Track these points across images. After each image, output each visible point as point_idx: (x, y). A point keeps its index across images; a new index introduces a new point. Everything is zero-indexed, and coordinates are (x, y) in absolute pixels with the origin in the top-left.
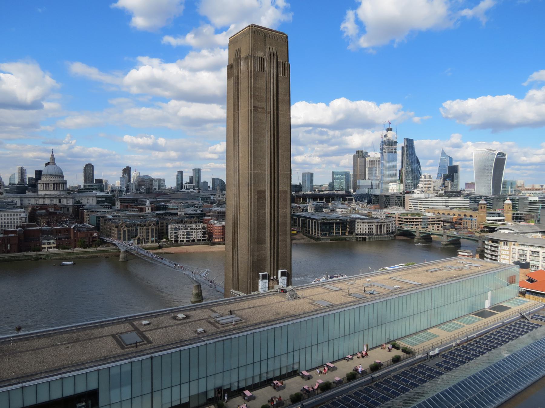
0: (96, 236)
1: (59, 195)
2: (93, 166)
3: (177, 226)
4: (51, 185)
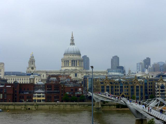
1: (75, 70)
2: (118, 58)
4: (70, 62)
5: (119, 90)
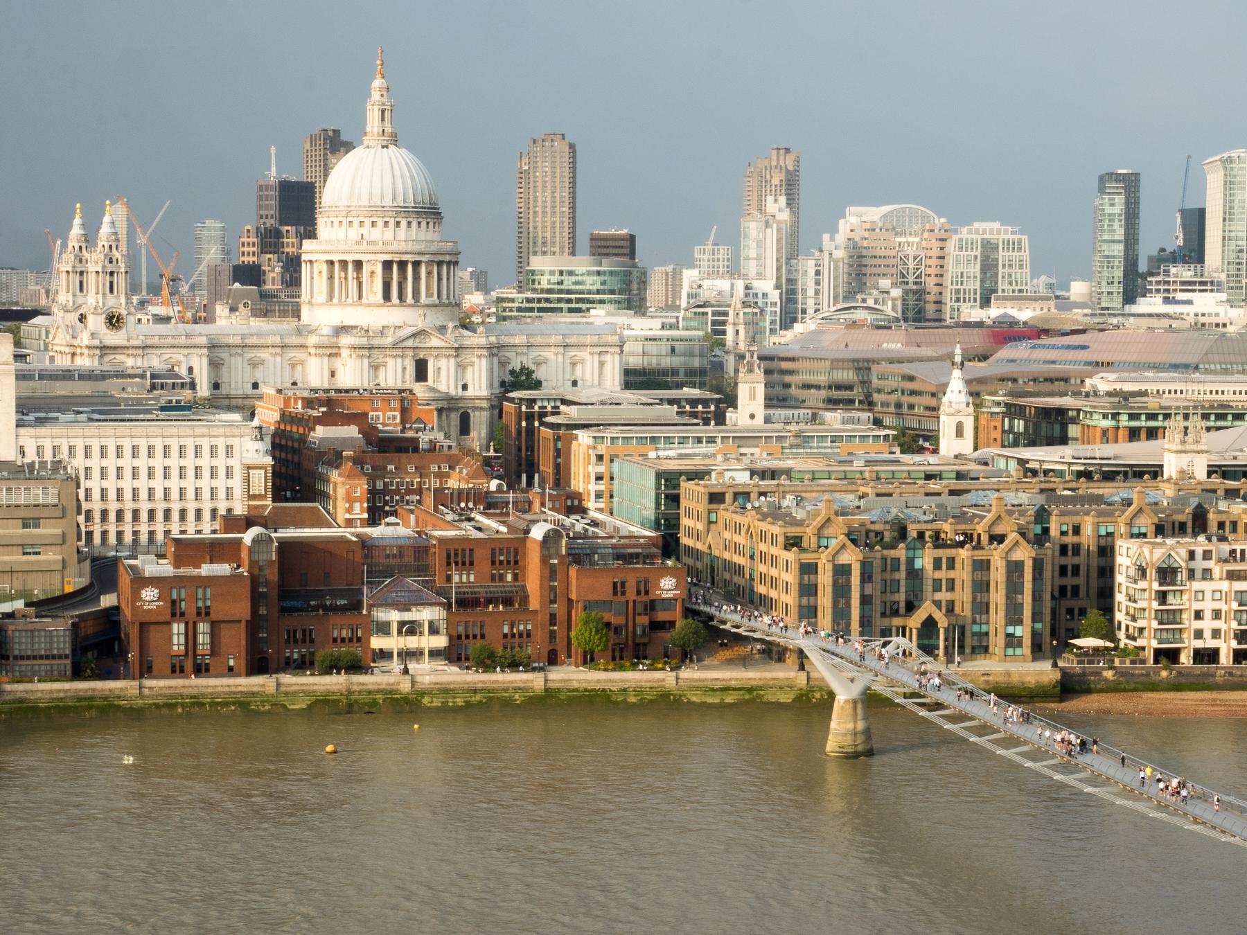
0: (670, 595)
1: (414, 335)
3: (1176, 549)
5: (903, 583)
